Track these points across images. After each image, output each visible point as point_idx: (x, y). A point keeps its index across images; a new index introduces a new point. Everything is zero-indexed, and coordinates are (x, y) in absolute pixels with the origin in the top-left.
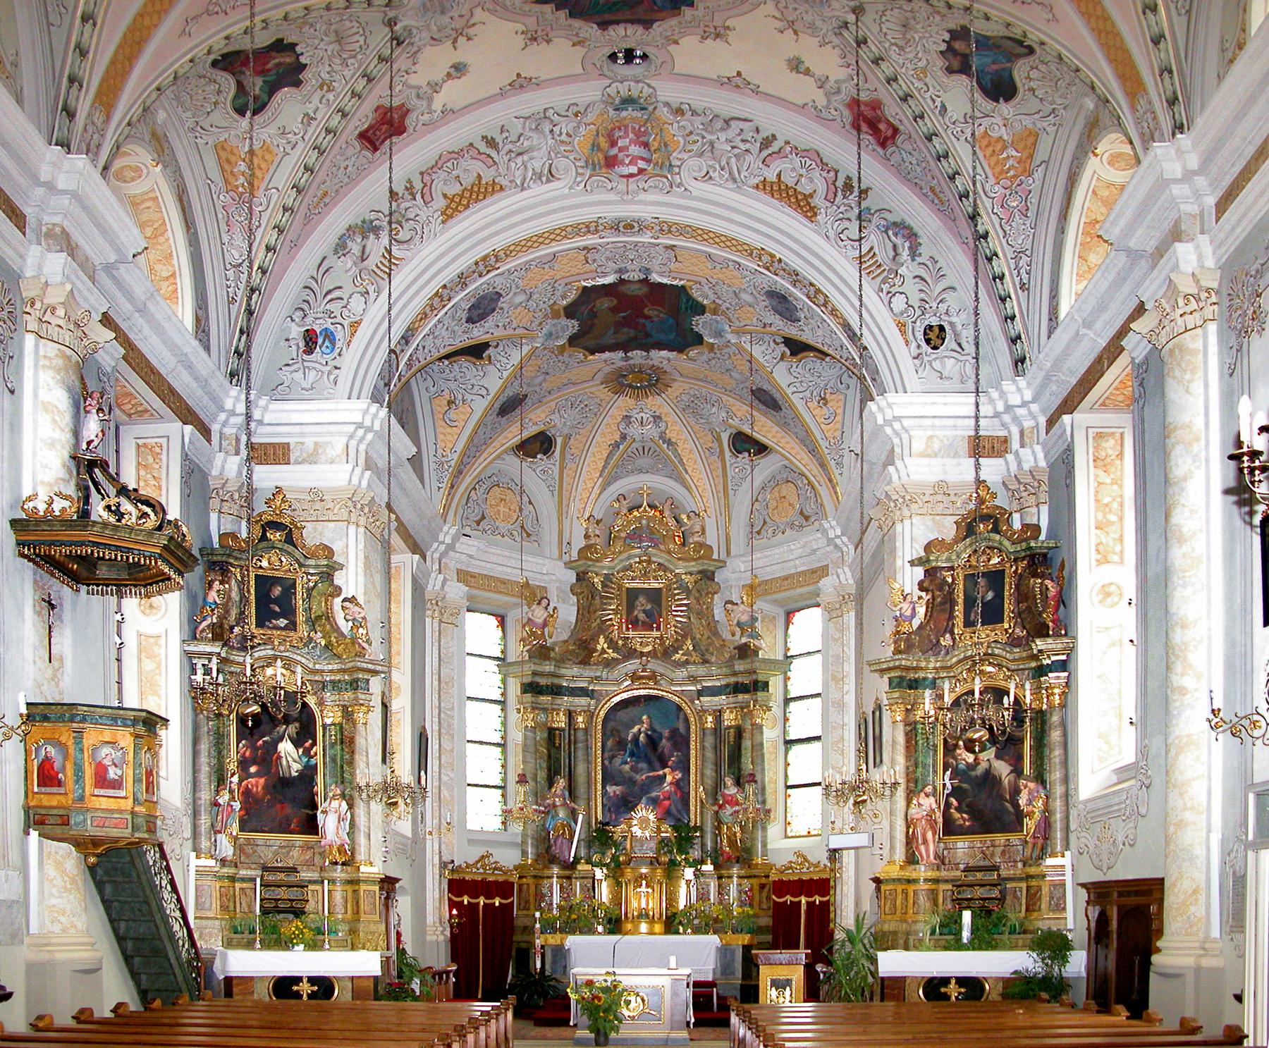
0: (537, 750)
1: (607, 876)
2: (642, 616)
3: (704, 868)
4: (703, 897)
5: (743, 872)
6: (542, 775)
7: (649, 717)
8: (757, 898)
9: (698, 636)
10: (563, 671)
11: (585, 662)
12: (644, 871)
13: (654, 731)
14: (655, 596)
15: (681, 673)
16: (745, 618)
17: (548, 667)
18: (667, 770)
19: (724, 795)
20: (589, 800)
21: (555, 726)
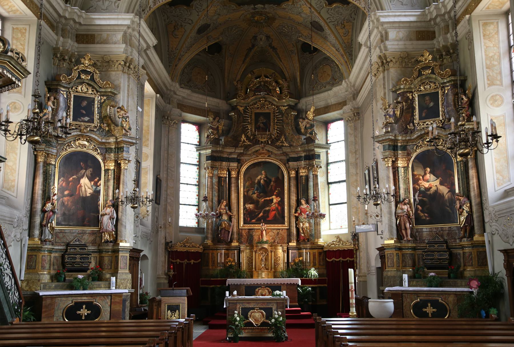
2: (262, 125)
7: (265, 172)
9: (287, 134)
14: (267, 116)
18: (274, 197)
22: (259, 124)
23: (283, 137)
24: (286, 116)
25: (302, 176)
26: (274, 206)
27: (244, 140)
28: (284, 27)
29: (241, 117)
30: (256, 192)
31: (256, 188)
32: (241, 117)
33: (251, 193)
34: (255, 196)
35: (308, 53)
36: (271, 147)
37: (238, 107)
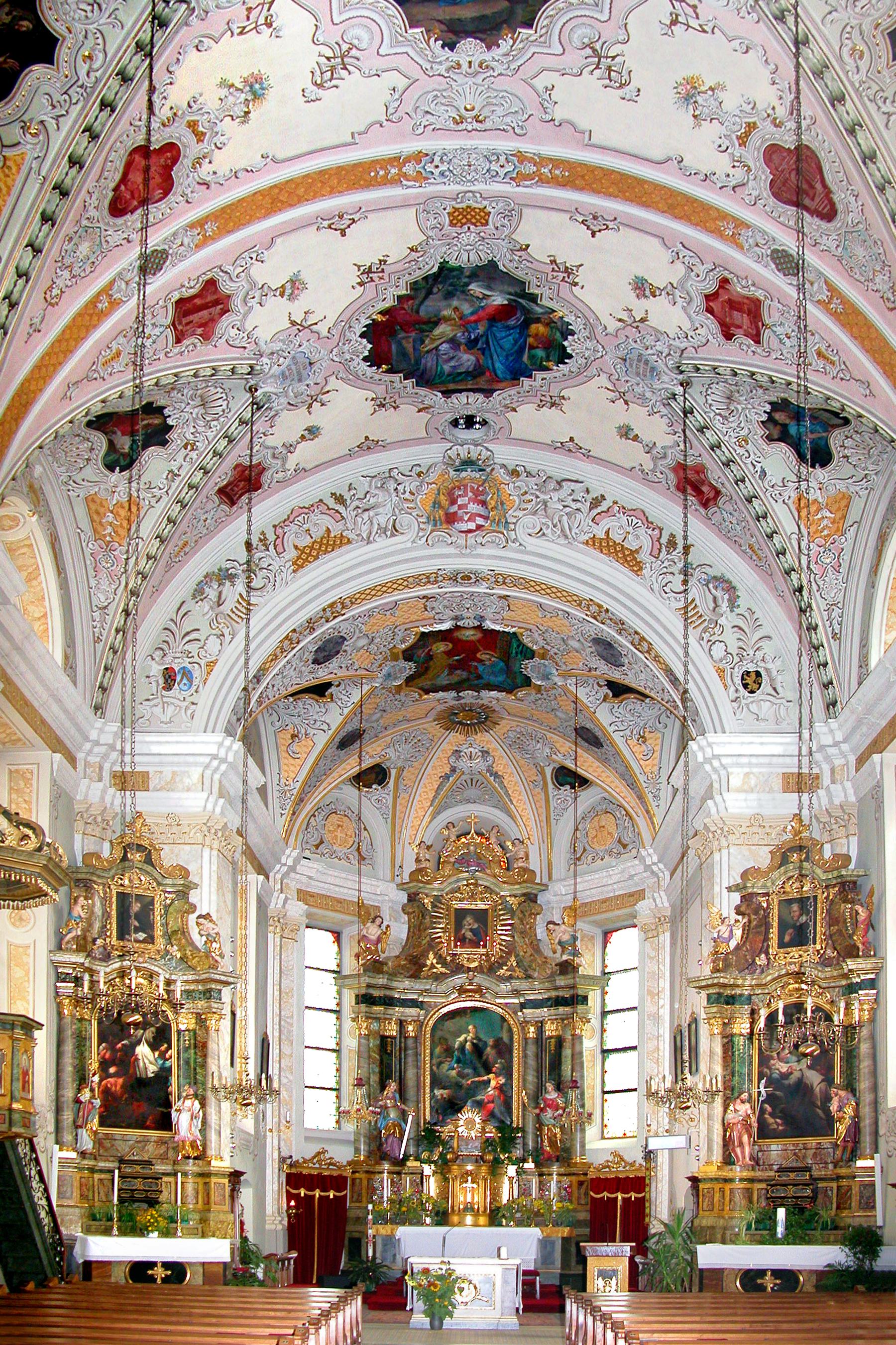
0: (370, 1057)
1: (435, 1172)
2: (469, 935)
3: (526, 1166)
4: (525, 1192)
5: (562, 1170)
6: (375, 1079)
8: (575, 1194)
9: (522, 953)
10: (395, 984)
11: (415, 976)
12: (470, 1167)
13: (480, 1040)
15: (505, 987)
16: (566, 937)
17: (381, 980)
18: (491, 1076)
19: (545, 1100)
20: (418, 1102)
21: (387, 1034)
23: (513, 959)
26: (491, 1091)
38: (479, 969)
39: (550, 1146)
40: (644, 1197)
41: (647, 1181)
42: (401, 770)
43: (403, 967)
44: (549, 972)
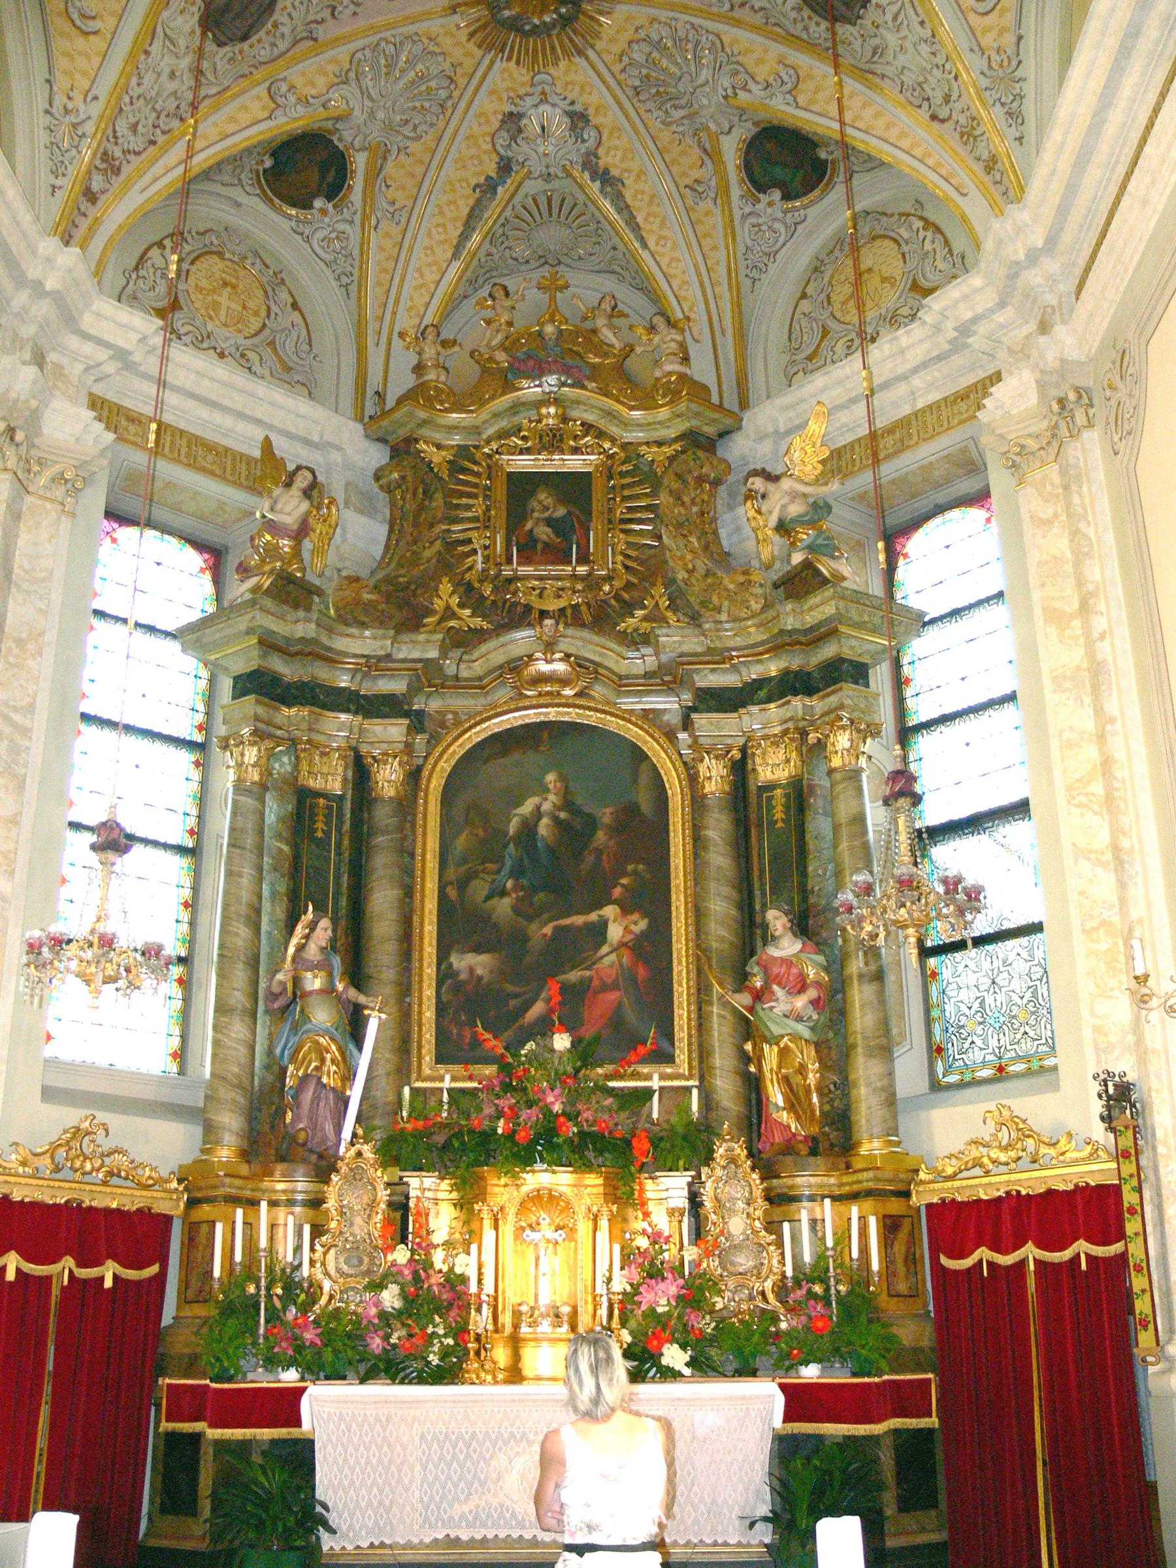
2: (544, 533)
7: (562, 777)
9: (681, 575)
10: (340, 644)
17: (301, 627)
18: (610, 911)
21: (316, 784)
22: (529, 525)
24: (675, 485)
25: (770, 787)
26: (608, 960)
27: (448, 607)
28: (658, 45)
29: (439, 496)
30: (510, 884)
31: (508, 863)
32: (439, 496)
33: (485, 892)
34: (503, 907)
35: (776, 194)
36: (596, 638)
37: (422, 446)
38: (571, 617)
39: (791, 1106)
40: (1123, 1257)
41: (1129, 1197)
42: (381, 154)
43: (368, 607)
44: (756, 606)
